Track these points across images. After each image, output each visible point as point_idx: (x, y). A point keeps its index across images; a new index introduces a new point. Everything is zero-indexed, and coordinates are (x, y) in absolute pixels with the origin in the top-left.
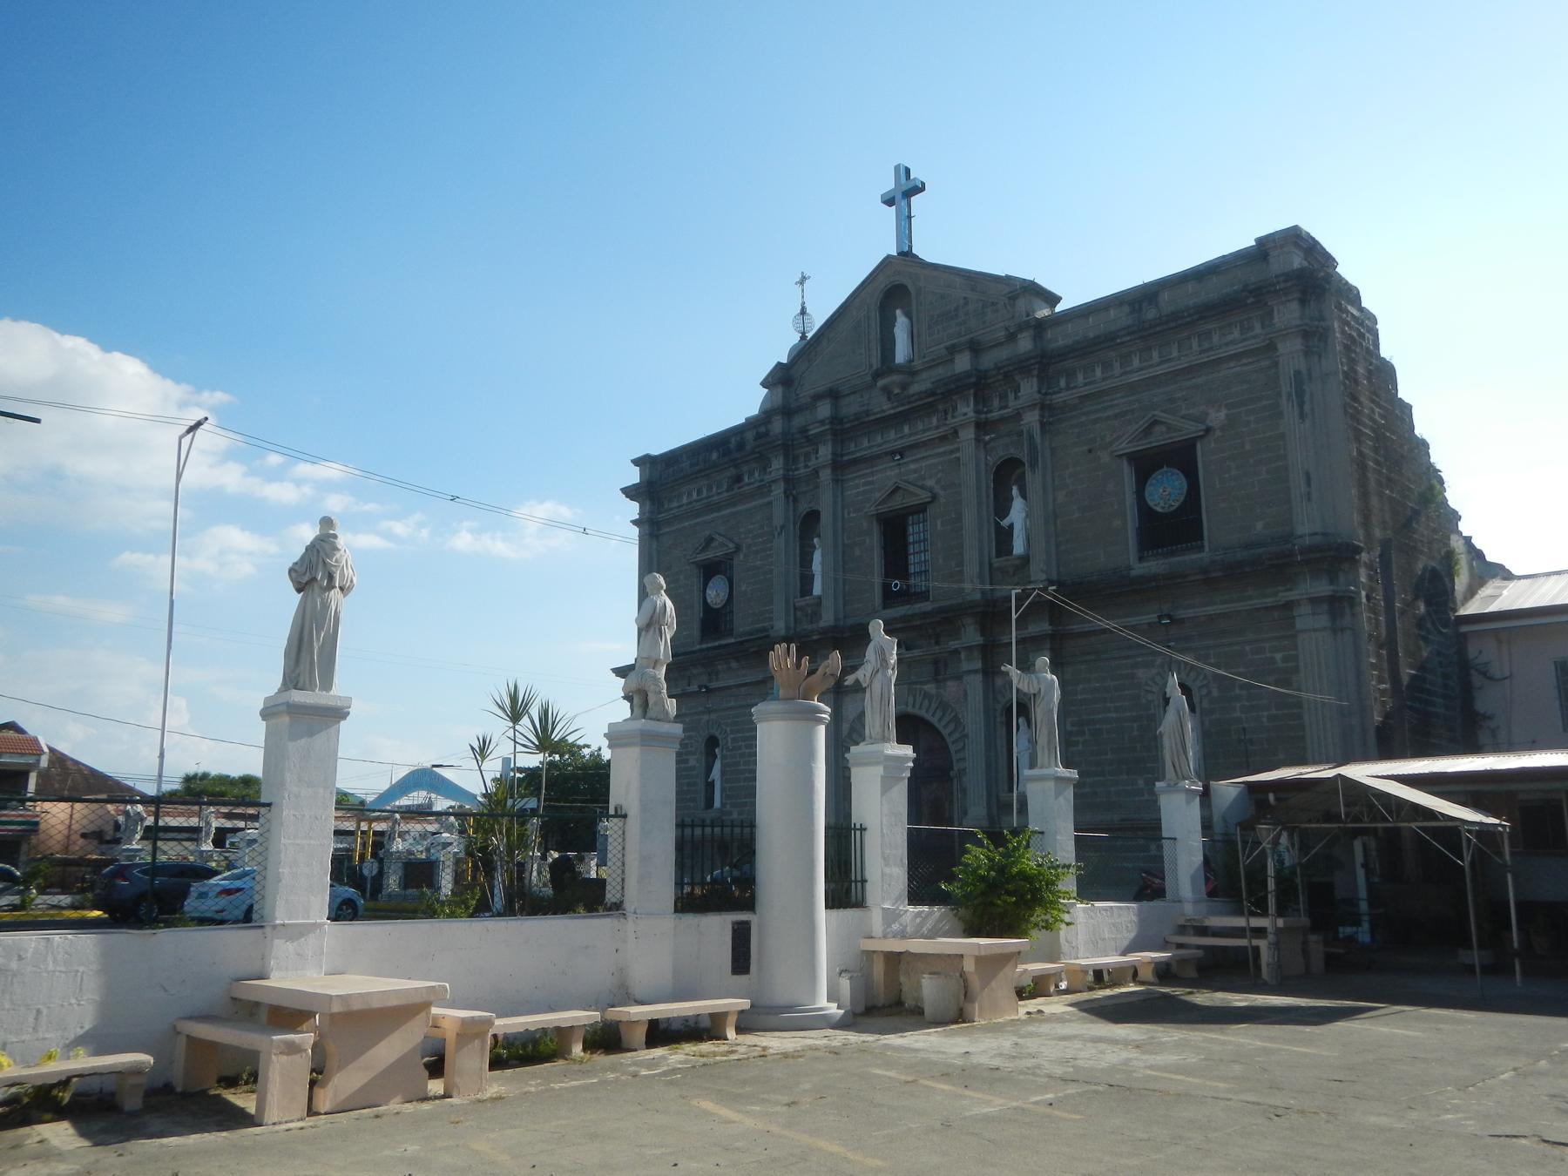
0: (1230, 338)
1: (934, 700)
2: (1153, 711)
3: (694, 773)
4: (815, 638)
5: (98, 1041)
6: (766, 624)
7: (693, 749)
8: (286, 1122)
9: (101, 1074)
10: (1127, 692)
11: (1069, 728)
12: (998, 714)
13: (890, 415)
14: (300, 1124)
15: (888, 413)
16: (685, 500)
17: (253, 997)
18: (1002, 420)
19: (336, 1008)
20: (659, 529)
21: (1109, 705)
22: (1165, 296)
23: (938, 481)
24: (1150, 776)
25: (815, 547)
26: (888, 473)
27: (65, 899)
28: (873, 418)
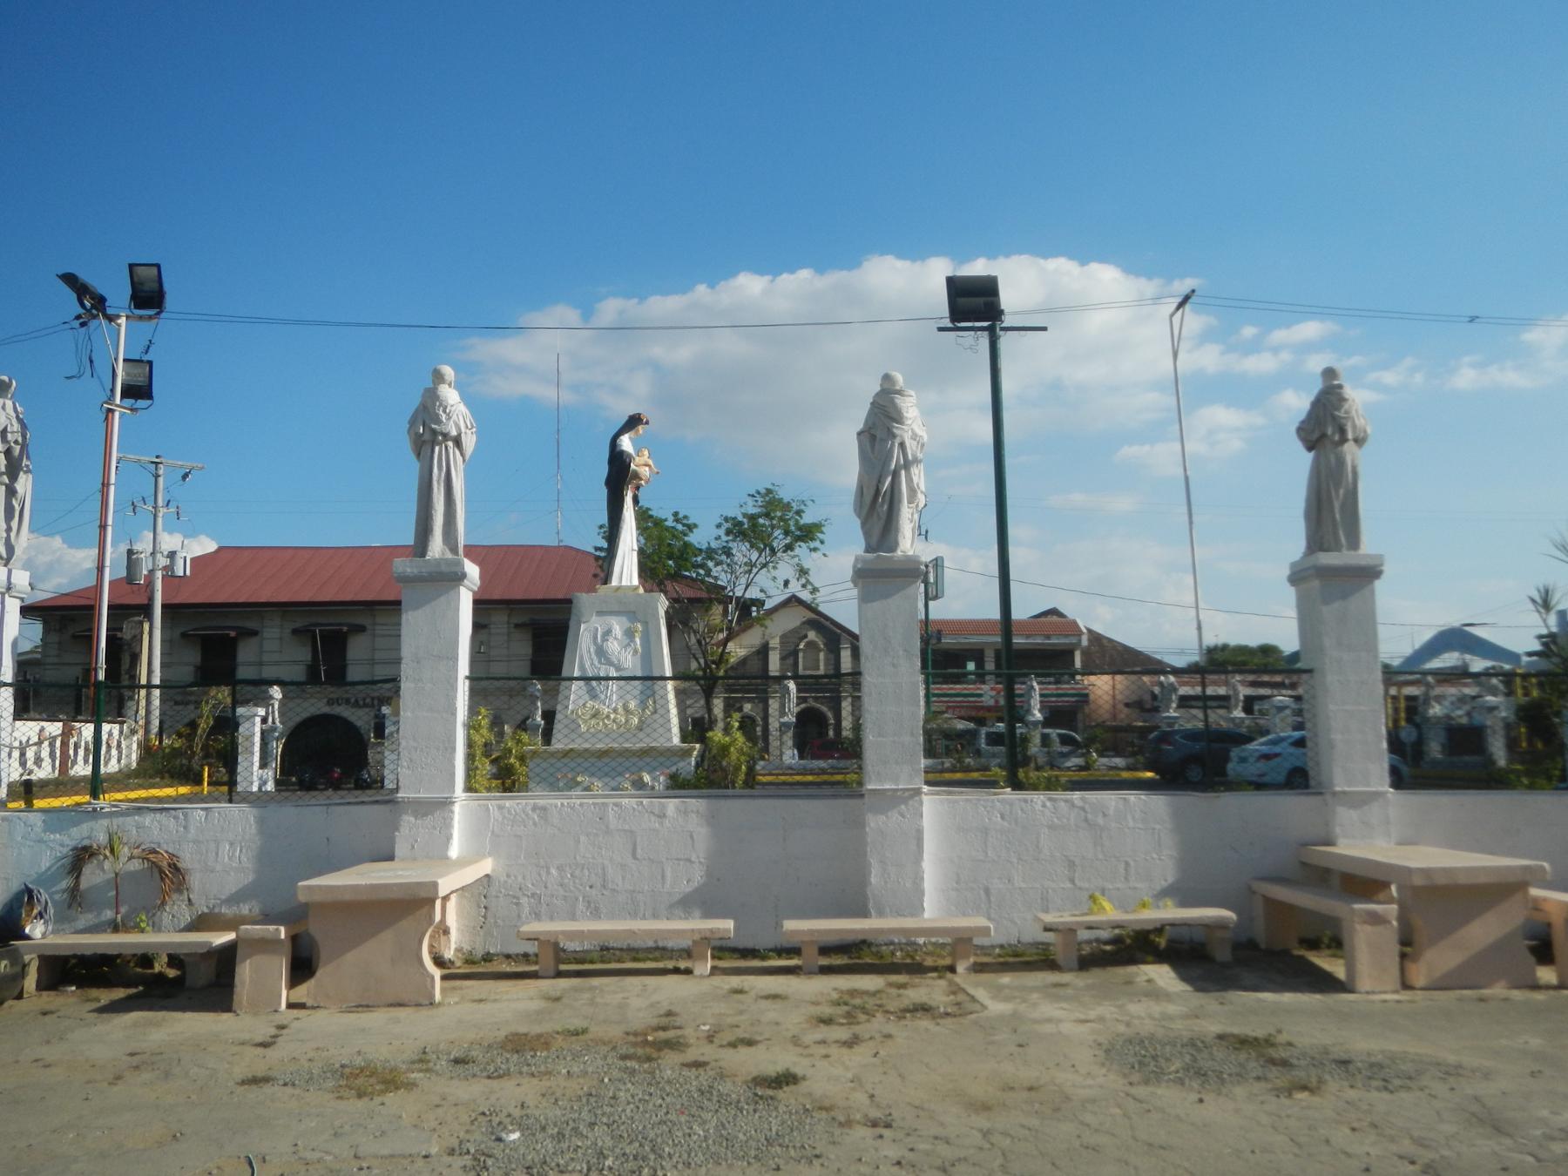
5: (1183, 893)
8: (1381, 992)
9: (1189, 925)
14: (1396, 997)
17: (1323, 863)
19: (1418, 881)
27: (1119, 761)
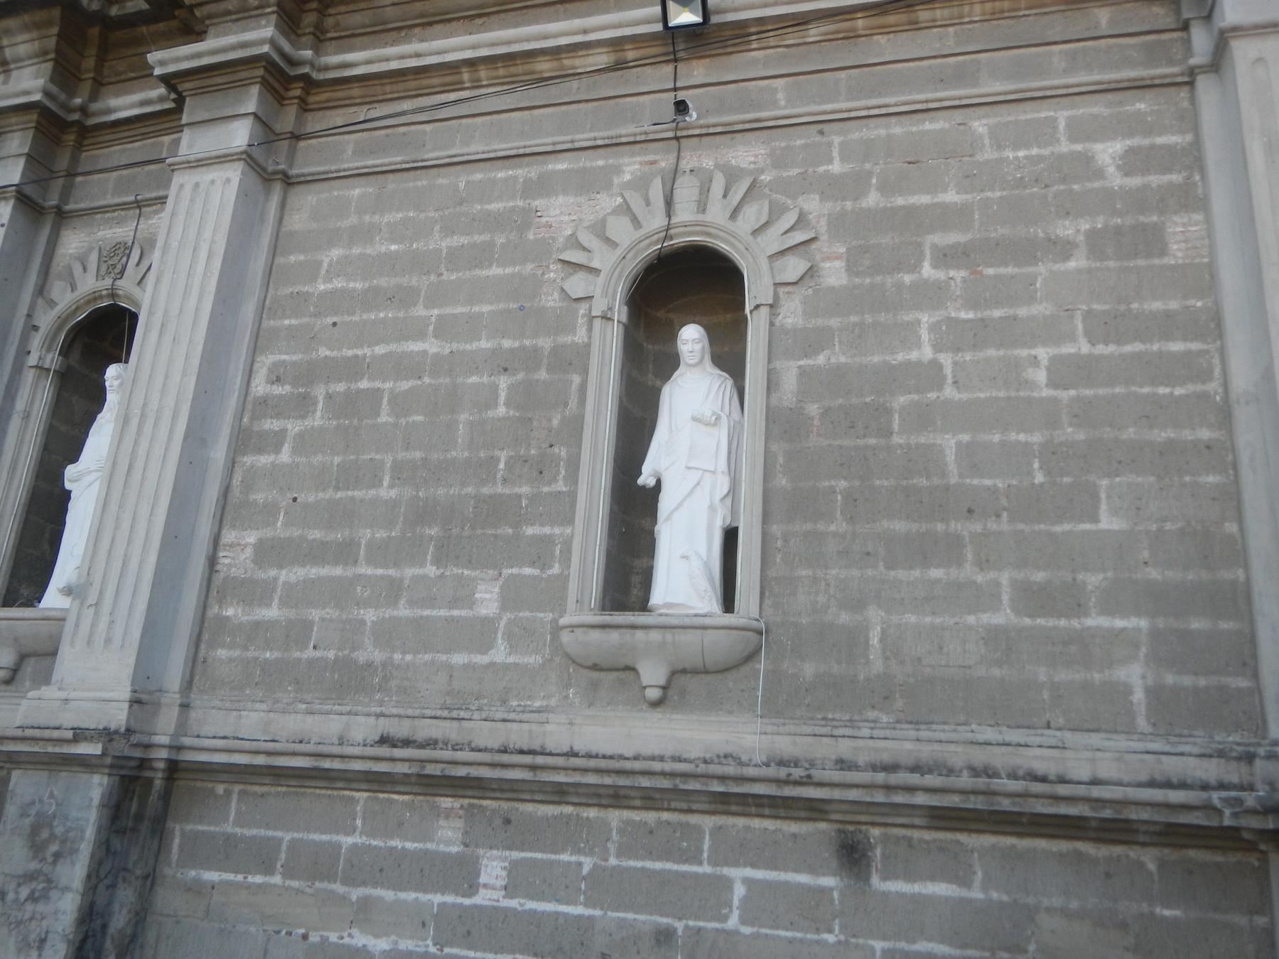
2: (580, 336)
10: (496, 271)
11: (260, 386)
12: (36, 342)
21: (420, 311)
24: (528, 571)
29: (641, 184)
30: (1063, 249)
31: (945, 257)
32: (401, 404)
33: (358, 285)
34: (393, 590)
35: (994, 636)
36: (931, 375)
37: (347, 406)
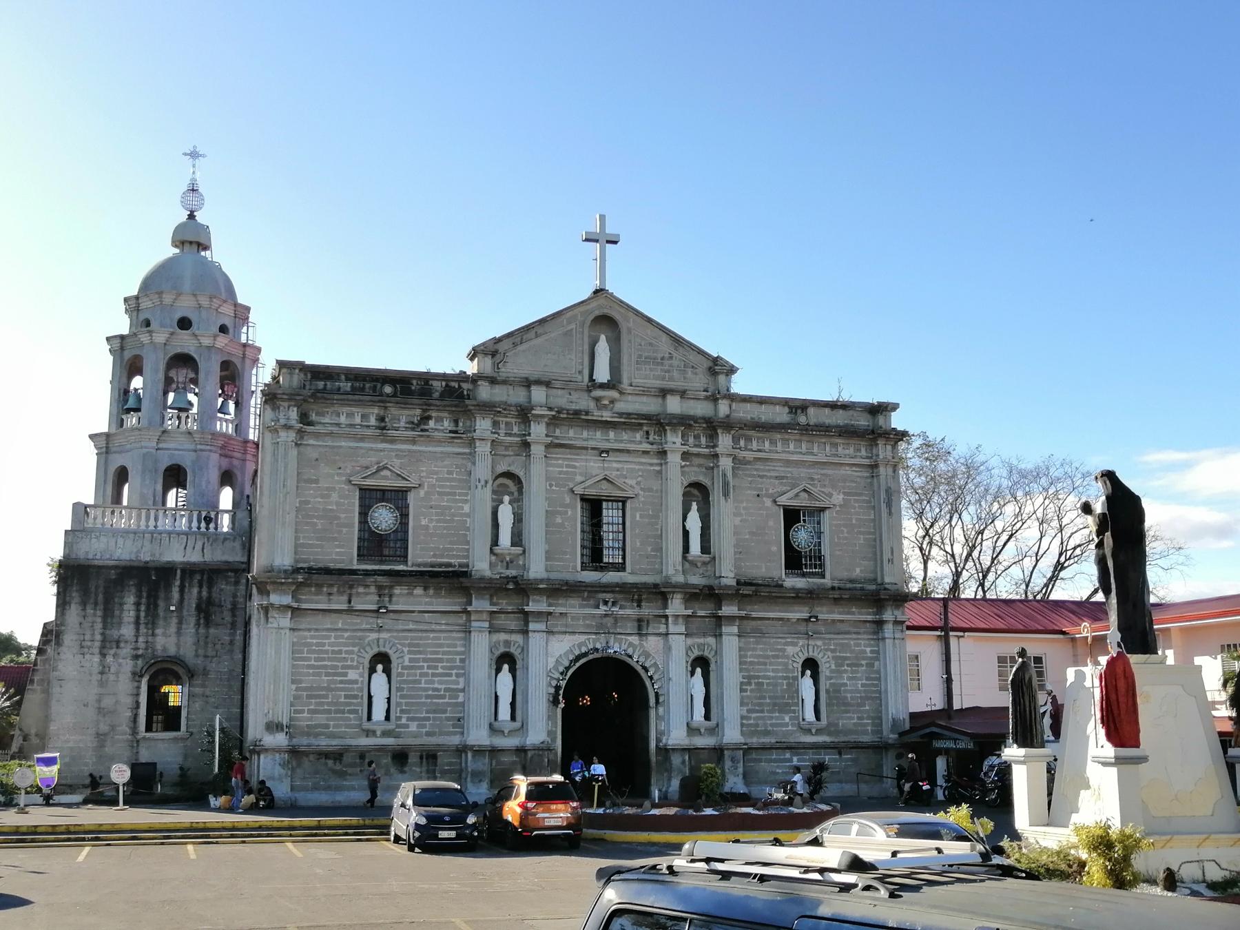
0: (847, 452)
1: (638, 648)
3: (355, 686)
4: (541, 586)
6: (453, 561)
7: (355, 664)
11: (742, 680)
13: (606, 421)
15: (604, 419)
16: (343, 419)
18: (698, 455)
20: (302, 438)
21: (768, 667)
22: (811, 411)
23: (638, 483)
25: (502, 502)
26: (592, 464)
28: (590, 418)
29: (803, 646)
30: (862, 665)
31: (848, 665)
32: (768, 684)
33: (756, 660)
34: (772, 718)
35: (854, 724)
36: (845, 685)
37: (758, 684)
